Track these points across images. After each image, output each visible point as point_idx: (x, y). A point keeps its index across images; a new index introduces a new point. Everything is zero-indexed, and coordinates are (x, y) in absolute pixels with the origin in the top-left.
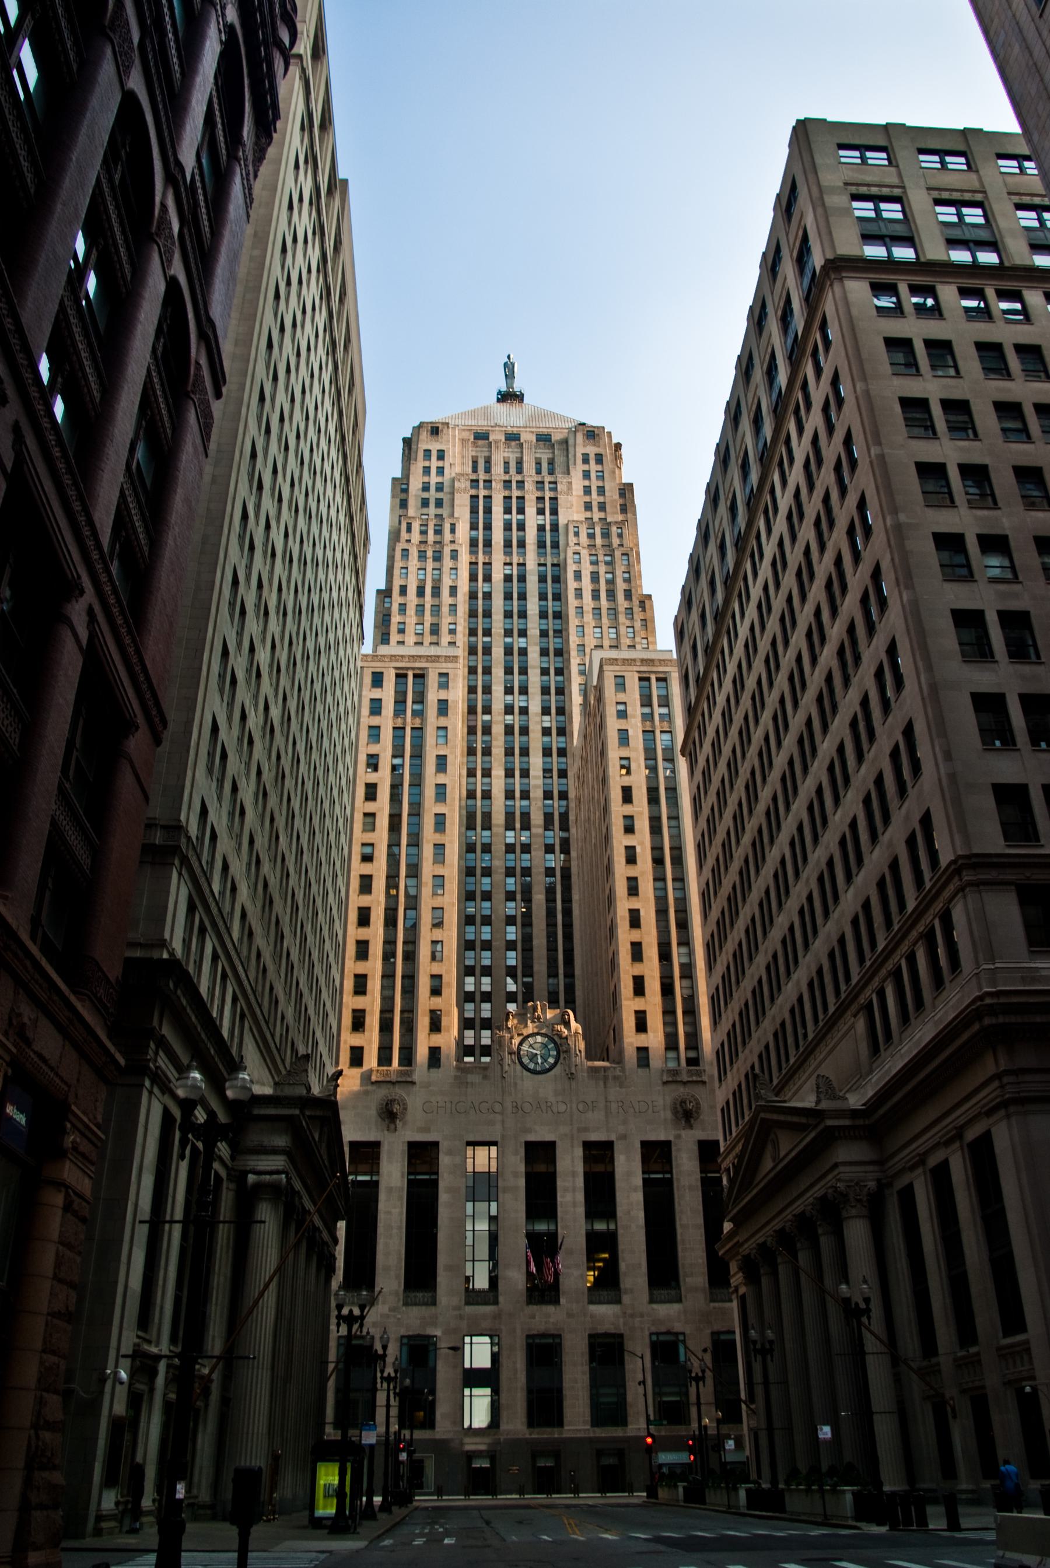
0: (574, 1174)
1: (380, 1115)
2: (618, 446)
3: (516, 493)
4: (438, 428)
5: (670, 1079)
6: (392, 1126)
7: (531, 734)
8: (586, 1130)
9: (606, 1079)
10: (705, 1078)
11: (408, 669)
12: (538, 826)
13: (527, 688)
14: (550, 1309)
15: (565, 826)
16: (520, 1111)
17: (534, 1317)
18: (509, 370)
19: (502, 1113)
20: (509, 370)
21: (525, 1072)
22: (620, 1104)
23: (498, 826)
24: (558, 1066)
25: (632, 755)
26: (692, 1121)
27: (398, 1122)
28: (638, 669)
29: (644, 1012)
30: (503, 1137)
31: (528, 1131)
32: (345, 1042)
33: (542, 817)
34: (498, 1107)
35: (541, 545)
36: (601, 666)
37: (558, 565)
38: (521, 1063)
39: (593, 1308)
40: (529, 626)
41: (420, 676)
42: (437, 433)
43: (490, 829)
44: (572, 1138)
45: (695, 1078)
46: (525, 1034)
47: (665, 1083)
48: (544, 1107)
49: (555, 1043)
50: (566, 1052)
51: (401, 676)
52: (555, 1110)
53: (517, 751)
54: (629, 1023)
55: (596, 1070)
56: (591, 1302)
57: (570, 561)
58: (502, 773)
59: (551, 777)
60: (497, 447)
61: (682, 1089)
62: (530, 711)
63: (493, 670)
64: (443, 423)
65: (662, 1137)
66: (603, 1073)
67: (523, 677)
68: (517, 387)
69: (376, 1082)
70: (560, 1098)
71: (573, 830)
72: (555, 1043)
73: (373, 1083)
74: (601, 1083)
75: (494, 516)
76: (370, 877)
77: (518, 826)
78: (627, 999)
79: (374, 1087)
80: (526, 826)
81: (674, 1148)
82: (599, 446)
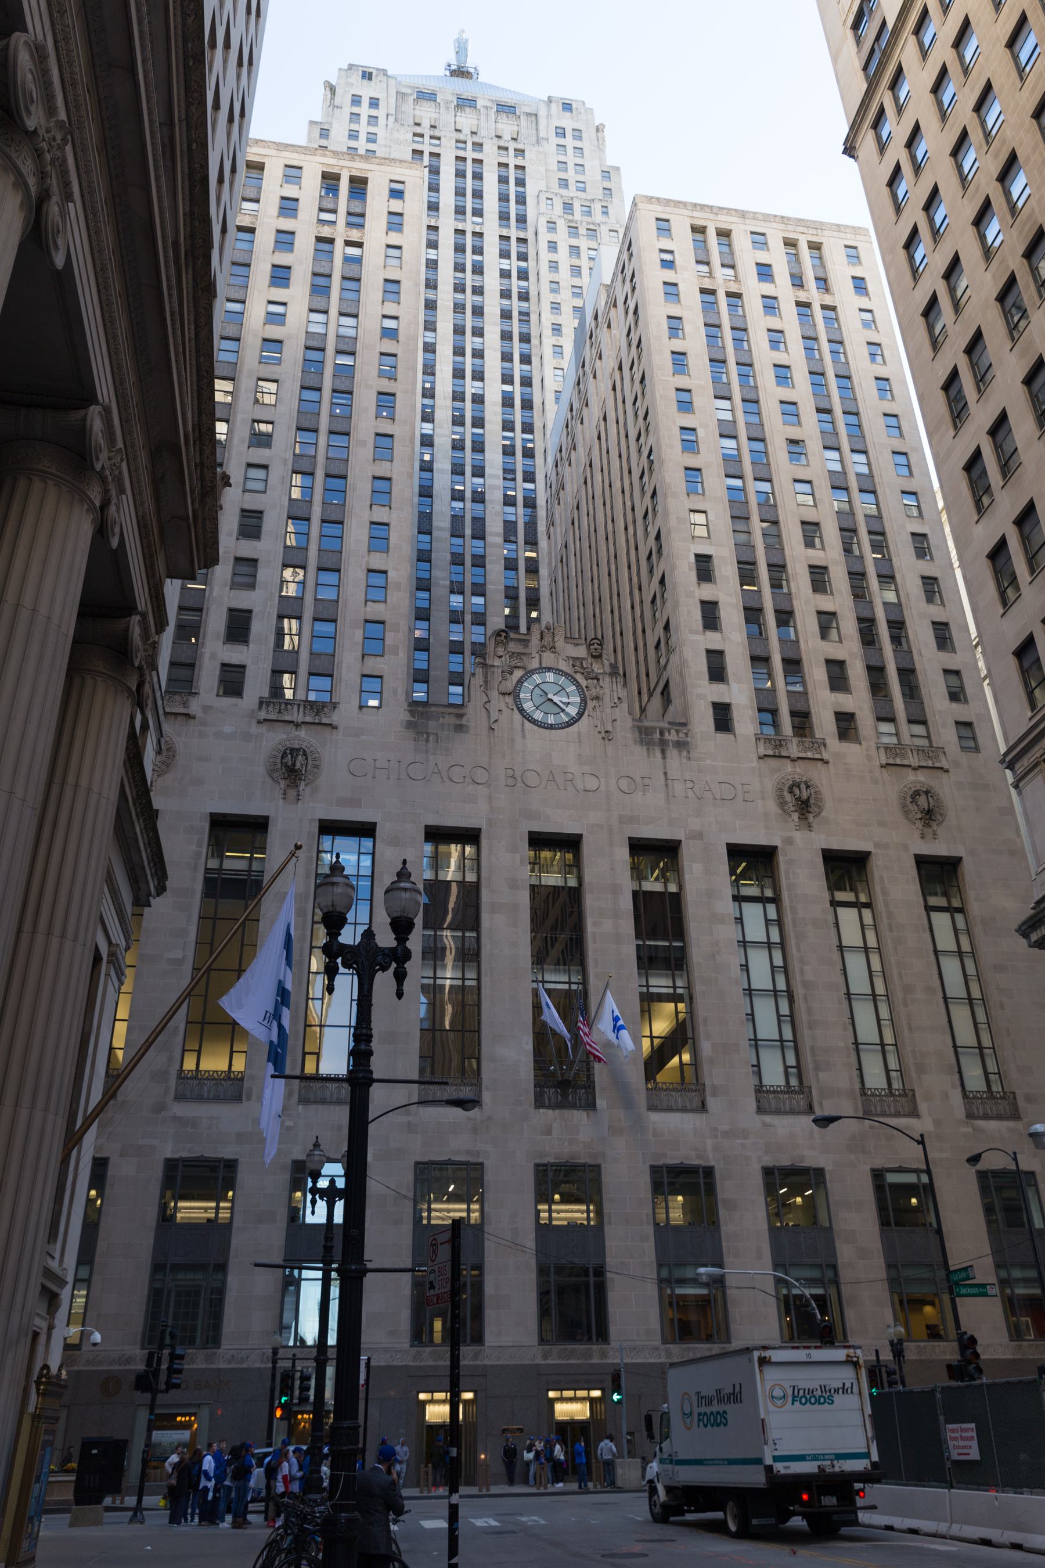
0: (616, 889)
1: (271, 773)
4: (370, 74)
5: (770, 753)
6: (292, 793)
9: (663, 744)
10: (825, 756)
12: (497, 535)
13: (483, 373)
14: (579, 1116)
15: (532, 542)
16: (520, 784)
17: (549, 1132)
18: (461, 49)
19: (487, 784)
20: (461, 49)
21: (527, 724)
22: (690, 785)
23: (441, 529)
26: (810, 816)
28: (689, 213)
29: (721, 653)
32: (213, 656)
34: (481, 776)
36: (634, 204)
38: (522, 711)
39: (655, 1117)
41: (359, 185)
42: (370, 79)
45: (809, 755)
50: (597, 698)
51: (330, 180)
52: (580, 787)
53: (468, 444)
54: (699, 665)
56: (652, 1108)
57: (543, 229)
58: (449, 467)
59: (514, 480)
60: (448, 108)
61: (788, 767)
64: (378, 69)
68: (470, 64)
70: (587, 769)
71: (543, 543)
73: (259, 722)
75: (442, 175)
76: (259, 514)
77: (468, 531)
78: (691, 632)
79: (263, 729)
80: (480, 534)
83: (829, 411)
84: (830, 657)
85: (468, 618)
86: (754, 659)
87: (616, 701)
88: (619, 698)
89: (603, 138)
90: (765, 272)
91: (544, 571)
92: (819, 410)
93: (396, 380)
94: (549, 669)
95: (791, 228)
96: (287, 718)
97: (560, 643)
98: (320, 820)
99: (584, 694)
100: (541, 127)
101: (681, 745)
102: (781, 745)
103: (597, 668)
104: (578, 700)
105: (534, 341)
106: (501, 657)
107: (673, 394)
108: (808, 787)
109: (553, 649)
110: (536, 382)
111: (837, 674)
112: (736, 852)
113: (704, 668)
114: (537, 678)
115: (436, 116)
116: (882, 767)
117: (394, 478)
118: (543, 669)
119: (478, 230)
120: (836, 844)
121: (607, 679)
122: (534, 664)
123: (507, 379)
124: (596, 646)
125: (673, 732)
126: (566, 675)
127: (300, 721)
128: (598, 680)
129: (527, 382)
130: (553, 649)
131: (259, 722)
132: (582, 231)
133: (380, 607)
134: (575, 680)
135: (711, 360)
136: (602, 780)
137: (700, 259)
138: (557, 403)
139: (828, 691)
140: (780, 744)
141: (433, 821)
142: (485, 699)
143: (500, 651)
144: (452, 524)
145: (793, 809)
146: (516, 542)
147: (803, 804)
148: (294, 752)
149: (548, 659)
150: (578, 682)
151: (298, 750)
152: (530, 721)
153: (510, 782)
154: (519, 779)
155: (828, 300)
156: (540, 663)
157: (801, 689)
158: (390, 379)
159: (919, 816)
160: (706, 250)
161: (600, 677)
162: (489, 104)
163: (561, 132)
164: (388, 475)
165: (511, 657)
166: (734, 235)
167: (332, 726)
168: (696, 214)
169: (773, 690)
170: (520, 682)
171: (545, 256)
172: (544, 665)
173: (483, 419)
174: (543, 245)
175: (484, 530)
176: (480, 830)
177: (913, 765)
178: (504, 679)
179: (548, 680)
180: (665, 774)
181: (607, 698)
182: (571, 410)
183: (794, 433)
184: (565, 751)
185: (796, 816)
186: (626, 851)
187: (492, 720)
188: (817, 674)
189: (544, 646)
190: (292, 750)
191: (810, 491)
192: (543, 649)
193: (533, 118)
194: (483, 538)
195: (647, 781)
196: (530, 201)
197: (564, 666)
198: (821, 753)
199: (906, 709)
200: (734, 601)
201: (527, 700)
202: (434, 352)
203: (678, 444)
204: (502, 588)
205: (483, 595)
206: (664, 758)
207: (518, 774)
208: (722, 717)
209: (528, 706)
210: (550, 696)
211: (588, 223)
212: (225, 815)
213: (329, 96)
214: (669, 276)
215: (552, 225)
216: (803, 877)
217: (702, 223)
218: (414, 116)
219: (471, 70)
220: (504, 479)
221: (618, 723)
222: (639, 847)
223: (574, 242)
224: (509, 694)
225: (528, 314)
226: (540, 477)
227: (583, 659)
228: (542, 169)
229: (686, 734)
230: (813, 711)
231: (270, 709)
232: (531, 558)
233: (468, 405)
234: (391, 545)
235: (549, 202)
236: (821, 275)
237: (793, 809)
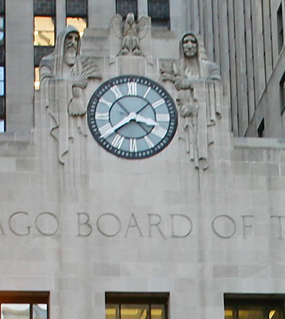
8: (230, 271)
9: (271, 172)
16: (95, 233)
19: (57, 236)
30: (60, 283)
31: (115, 271)
34: (49, 224)
38: (96, 135)
44: (202, 286)
46: (105, 79)
48: (143, 223)
49: (167, 98)
50: (190, 115)
52: (167, 232)
72: (167, 98)
74: (262, 181)
87: (214, 117)
88: (217, 114)
94: (131, 78)
99: (174, 109)
103: (190, 76)
104: (167, 118)
106: (72, 65)
109: (135, 49)
114: (116, 91)
118: (122, 80)
121: (204, 89)
124: (190, 44)
128: (192, 90)
130: (135, 49)
134: (164, 91)
136: (194, 222)
142: (52, 125)
143: (71, 57)
149: (131, 64)
150: (167, 94)
153: (84, 230)
154: (94, 227)
170: (96, 97)
176: (49, 293)
178: (76, 96)
179: (130, 93)
180: (271, 209)
181: (202, 115)
184: (151, 186)
187: (61, 153)
192: (125, 49)
195: (248, 221)
201: (103, 122)
206: (270, 189)
207: (93, 220)
209: (106, 131)
221: (215, 147)
224: (82, 116)
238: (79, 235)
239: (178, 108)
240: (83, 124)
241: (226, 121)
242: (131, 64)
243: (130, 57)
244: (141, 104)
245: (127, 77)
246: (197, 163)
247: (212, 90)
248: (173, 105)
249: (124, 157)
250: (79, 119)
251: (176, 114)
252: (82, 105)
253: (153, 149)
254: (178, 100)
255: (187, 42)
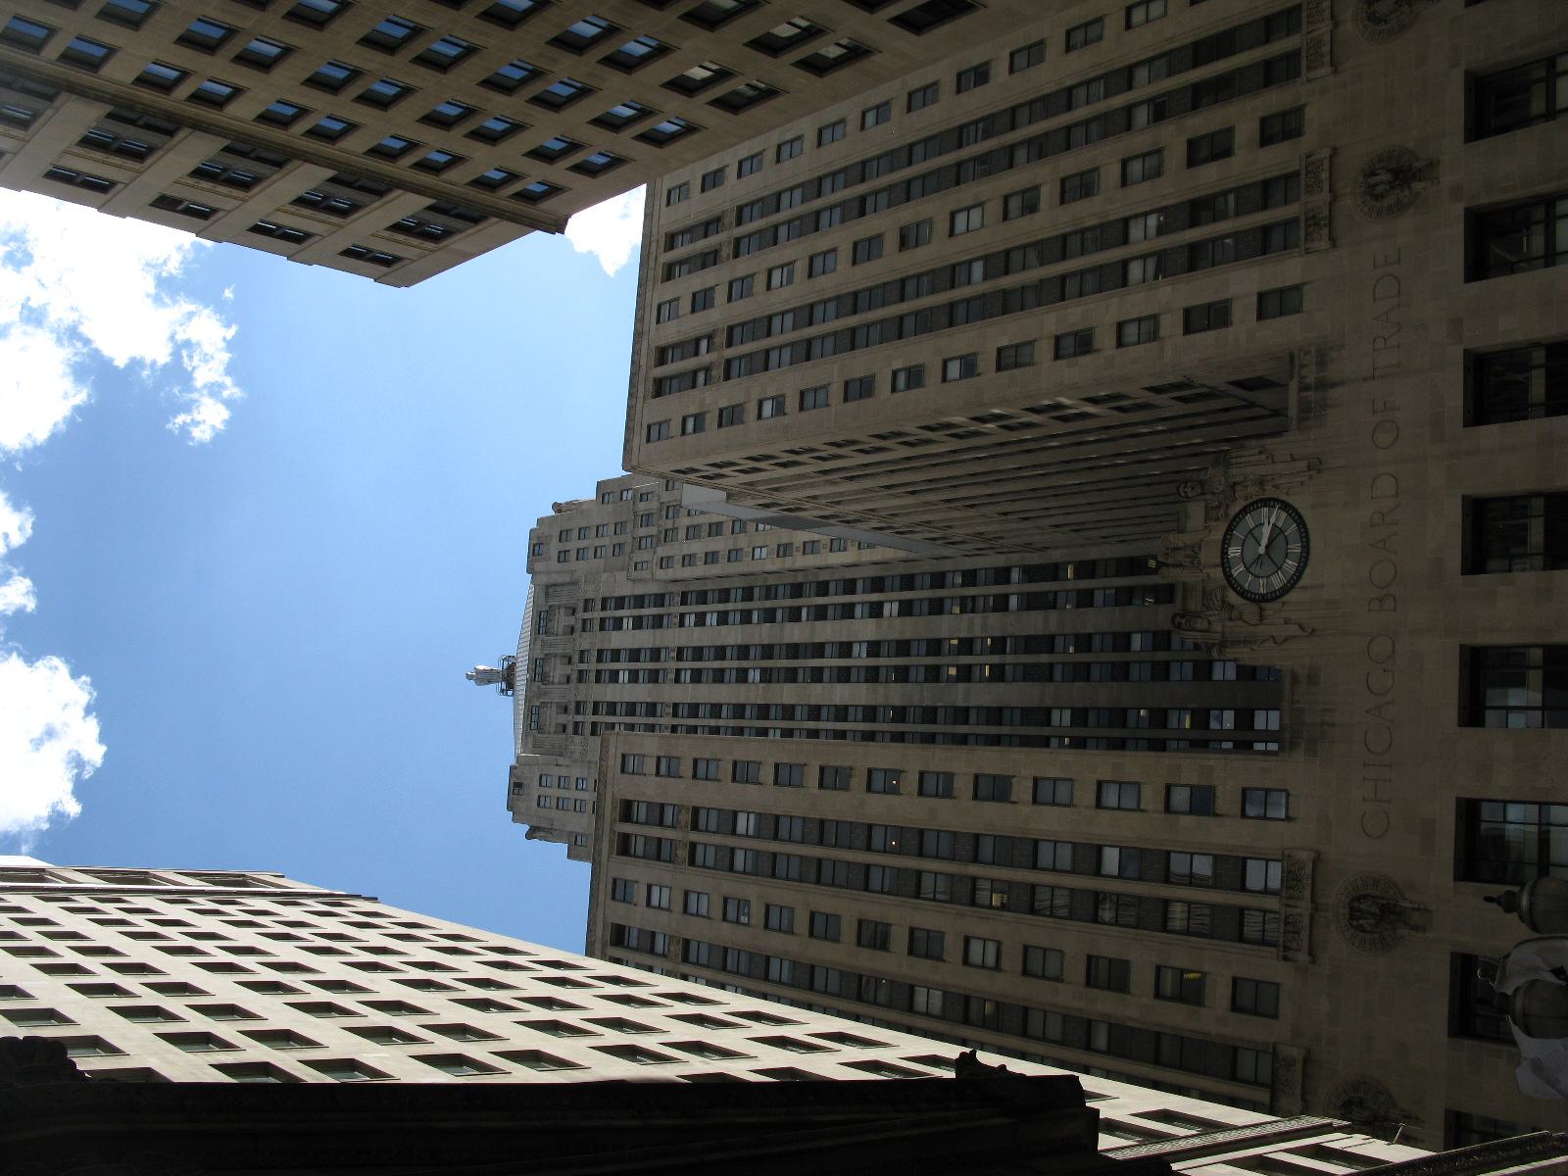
2: (557, 507)
3: (592, 666)
5: (1325, 231)
7: (907, 636)
9: (1323, 385)
10: (1325, 153)
11: (612, 831)
13: (841, 644)
15: (1053, 572)
18: (484, 678)
20: (484, 678)
21: (1304, 581)
24: (1295, 500)
25: (755, 396)
27: (1407, 904)
28: (641, 400)
29: (1187, 312)
33: (1033, 613)
35: (658, 622)
37: (684, 595)
38: (1285, 590)
40: (756, 641)
43: (1048, 711)
45: (1325, 176)
46: (1225, 582)
47: (1333, 241)
49: (1245, 511)
54: (1206, 341)
55: (1305, 410)
57: (669, 574)
60: (546, 693)
62: (874, 638)
63: (813, 702)
65: (1457, 232)
66: (1310, 393)
67: (828, 650)
69: (1310, 953)
71: (1055, 556)
72: (1245, 511)
73: (1313, 962)
74: (1334, 393)
77: (1044, 658)
81: (1484, 200)
82: (551, 536)
83: (863, 199)
84: (1184, 162)
85: (1161, 656)
86: (1192, 267)
87: (1264, 457)
88: (1260, 453)
89: (567, 503)
90: (702, 301)
91: (1093, 553)
92: (862, 213)
93: (851, 768)
94: (1224, 553)
95: (651, 275)
96: (1306, 921)
97: (1187, 539)
98: (1457, 878)
99: (1256, 502)
100: (560, 581)
101: (1322, 362)
102: (1314, 217)
105: (800, 579)
106: (1209, 622)
107: (852, 405)
108: (1373, 174)
109: (1194, 550)
110: (849, 574)
111: (1209, 149)
112: (1478, 268)
113: (1209, 336)
114: (1238, 570)
115: (554, 707)
116: (1335, 72)
117: (974, 770)
118: (1225, 563)
119: (674, 654)
120: (1455, 121)
121: (1234, 471)
122: (1218, 573)
123: (847, 612)
124: (1188, 490)
125: (1303, 373)
126: (1230, 530)
127: (1310, 905)
128: (1235, 483)
129: (850, 587)
131: (1313, 962)
132: (669, 524)
133: (1147, 791)
135: (808, 359)
137: (690, 383)
138: (874, 546)
139: (1233, 158)
140: (1313, 221)
141: (1451, 713)
142: (1270, 643)
144: (1033, 680)
145: (1407, 192)
146: (1056, 593)
147: (1398, 177)
148: (1354, 915)
149: (1209, 555)
150: (1239, 513)
151: (1352, 909)
152: (1299, 578)
155: (731, 218)
156: (1216, 566)
157: (1231, 198)
158: (851, 776)
159: (1406, 8)
160: (679, 376)
161: (1231, 481)
162: (539, 642)
163: (563, 557)
164: (971, 780)
165: (1209, 608)
166: (662, 343)
167: (1318, 859)
168: (640, 394)
169: (1235, 235)
171: (700, 570)
172: (1219, 561)
173: (899, 642)
174: (687, 573)
175: (1043, 637)
177: (1329, 28)
180: (1365, 379)
181: (1262, 470)
182: (881, 529)
183: (891, 242)
185: (1417, 186)
186: (1483, 430)
187: (1300, 632)
188: (1210, 177)
189: (1192, 563)
190: (1352, 917)
191: (965, 214)
193: (551, 590)
194: (1052, 638)
196: (639, 590)
197: (1218, 535)
198: (1321, 161)
199: (1250, 48)
200: (1115, 300)
202: (819, 707)
203: (914, 393)
204: (1117, 609)
205: (1128, 636)
206: (1342, 383)
208: (1274, 303)
209: (1278, 581)
210: (1262, 550)
211: (660, 517)
212: (1451, 1015)
213: (542, 834)
214: (711, 420)
215: (665, 562)
216: (1511, 165)
217: (650, 385)
218: (556, 732)
219: (506, 664)
220: (973, 611)
222: (1479, 412)
223: (682, 534)
225: (768, 588)
226: (969, 564)
227: (1206, 506)
228: (604, 577)
229: (1306, 354)
230: (1261, 177)
231: (1294, 945)
232: (1076, 570)
233: (882, 661)
234: (1062, 776)
235: (639, 566)
236: (701, 231)
237: (1407, 192)
238: (1395, 610)
239: (1255, 498)
240: (1270, 608)
241: (1270, 443)
242: (1209, 555)
243: (1202, 556)
244: (1250, 541)
245: (1222, 559)
246: (1313, 473)
247: (1234, 461)
248: (1252, 504)
249: (1307, 558)
250: (1266, 613)
251: (1260, 500)
252: (1250, 610)
253: (1298, 525)
254: (1246, 499)
255: (1186, 492)
